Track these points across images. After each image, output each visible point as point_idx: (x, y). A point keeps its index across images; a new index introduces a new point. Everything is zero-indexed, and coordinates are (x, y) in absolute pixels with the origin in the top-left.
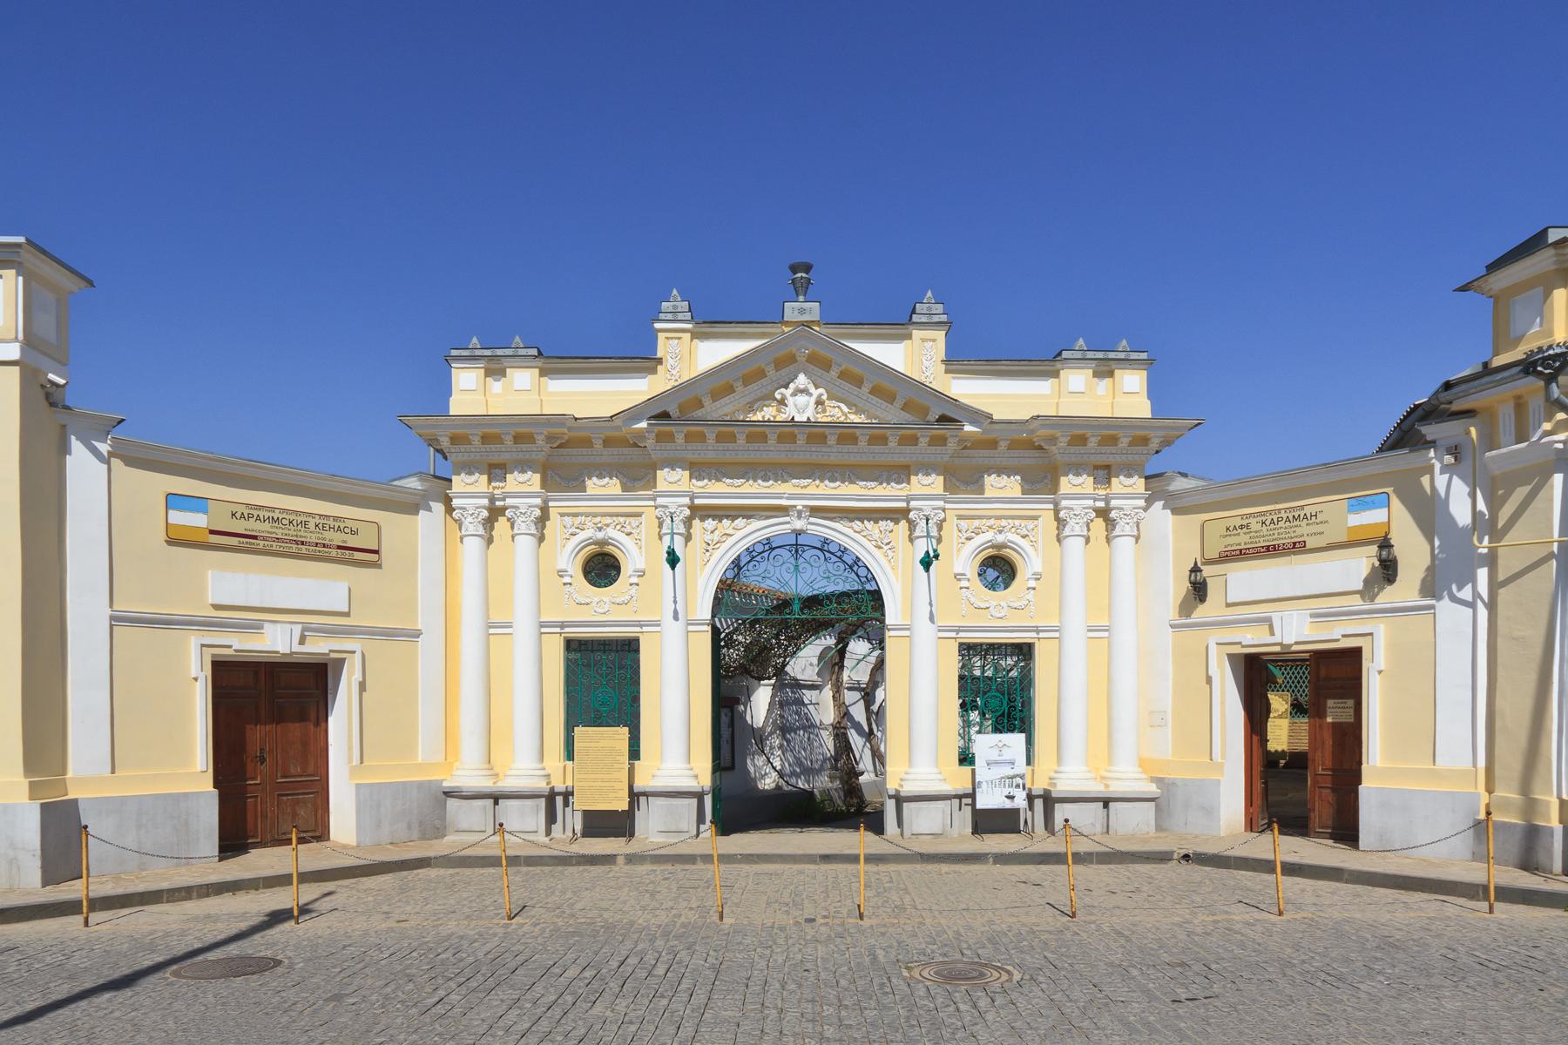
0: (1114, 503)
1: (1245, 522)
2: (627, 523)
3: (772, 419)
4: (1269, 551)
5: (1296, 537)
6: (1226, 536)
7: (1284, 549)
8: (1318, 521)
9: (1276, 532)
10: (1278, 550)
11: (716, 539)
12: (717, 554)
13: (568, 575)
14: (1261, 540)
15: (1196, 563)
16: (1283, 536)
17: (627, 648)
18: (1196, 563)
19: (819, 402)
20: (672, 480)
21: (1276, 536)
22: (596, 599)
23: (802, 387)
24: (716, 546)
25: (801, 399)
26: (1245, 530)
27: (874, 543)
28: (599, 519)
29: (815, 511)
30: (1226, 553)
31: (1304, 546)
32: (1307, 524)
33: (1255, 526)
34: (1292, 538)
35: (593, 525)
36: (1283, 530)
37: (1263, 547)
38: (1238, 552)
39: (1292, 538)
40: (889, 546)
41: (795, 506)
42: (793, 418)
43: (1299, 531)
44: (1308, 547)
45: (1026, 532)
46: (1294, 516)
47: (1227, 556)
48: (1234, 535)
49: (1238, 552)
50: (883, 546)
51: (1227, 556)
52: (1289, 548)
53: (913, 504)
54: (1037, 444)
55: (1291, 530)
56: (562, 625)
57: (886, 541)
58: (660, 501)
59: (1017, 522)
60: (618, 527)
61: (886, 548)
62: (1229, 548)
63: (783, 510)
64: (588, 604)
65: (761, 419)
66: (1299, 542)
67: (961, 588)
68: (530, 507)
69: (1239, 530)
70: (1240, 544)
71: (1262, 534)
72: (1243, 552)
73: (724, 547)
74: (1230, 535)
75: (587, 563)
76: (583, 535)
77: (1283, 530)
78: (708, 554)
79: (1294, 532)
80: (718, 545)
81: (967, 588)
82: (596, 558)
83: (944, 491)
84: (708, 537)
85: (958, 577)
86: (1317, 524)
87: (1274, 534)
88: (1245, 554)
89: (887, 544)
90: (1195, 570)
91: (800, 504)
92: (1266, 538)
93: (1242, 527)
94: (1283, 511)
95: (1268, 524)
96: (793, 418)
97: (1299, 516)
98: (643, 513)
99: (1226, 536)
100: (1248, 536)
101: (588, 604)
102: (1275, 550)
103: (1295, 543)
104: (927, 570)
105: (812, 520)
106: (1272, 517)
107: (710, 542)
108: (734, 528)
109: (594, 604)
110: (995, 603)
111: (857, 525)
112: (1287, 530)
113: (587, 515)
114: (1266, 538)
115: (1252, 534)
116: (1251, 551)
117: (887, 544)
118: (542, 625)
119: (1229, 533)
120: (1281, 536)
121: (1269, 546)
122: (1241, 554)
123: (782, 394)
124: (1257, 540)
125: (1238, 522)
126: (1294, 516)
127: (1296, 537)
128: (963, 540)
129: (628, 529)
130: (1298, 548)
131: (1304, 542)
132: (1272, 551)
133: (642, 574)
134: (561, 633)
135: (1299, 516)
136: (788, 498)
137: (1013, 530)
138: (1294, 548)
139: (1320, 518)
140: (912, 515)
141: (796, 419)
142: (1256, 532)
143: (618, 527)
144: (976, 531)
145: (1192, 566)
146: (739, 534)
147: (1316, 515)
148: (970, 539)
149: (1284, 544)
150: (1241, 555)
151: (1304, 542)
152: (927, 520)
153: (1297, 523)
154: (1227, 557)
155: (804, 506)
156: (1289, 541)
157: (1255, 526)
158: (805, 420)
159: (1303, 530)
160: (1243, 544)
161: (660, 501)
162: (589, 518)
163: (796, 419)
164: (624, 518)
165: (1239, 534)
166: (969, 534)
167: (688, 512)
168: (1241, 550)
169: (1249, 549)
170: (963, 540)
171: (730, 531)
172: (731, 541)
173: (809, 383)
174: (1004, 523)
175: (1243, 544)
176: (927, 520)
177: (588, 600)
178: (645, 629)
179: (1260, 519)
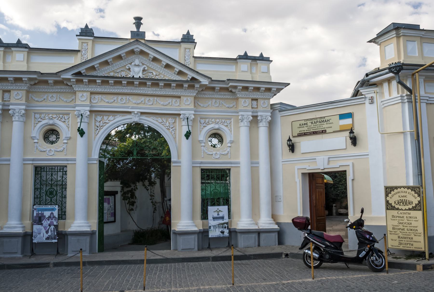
0: (259, 114)
1: (306, 122)
2: (63, 117)
3: (125, 76)
4: (314, 133)
5: (323, 128)
6: (300, 127)
7: (319, 133)
8: (330, 123)
9: (316, 126)
10: (317, 133)
11: (101, 125)
12: (102, 131)
13: (36, 139)
14: (311, 129)
15: (289, 138)
16: (319, 128)
17: (62, 170)
18: (289, 138)
19: (144, 70)
20: (82, 100)
21: (316, 128)
22: (48, 149)
23: (137, 64)
24: (101, 128)
25: (137, 69)
26: (306, 125)
27: (166, 127)
28: (51, 115)
29: (142, 113)
31: (326, 132)
32: (326, 124)
33: (309, 124)
34: (322, 129)
35: (48, 118)
36: (318, 126)
37: (312, 132)
38: (304, 134)
39: (322, 129)
40: (172, 129)
41: (134, 112)
42: (133, 76)
43: (324, 126)
44: (327, 132)
45: (227, 125)
46: (322, 121)
47: (300, 135)
48: (302, 127)
49: (304, 134)
50: (170, 129)
51: (300, 135)
52: (321, 133)
53: (181, 112)
54: (230, 90)
55: (321, 126)
56: (33, 160)
57: (171, 127)
58: (77, 108)
59: (223, 121)
60: (59, 119)
61: (171, 130)
62: (301, 132)
63: (130, 113)
64: (45, 151)
65: (120, 76)
66: (324, 130)
67: (202, 146)
68: (20, 109)
69: (304, 125)
70: (304, 131)
71: (311, 127)
72: (306, 133)
73: (105, 128)
74: (301, 127)
75: (46, 133)
76: (44, 122)
77: (318, 126)
78: (97, 131)
79: (322, 126)
80: (102, 127)
81: (204, 146)
82: (50, 132)
83: (194, 107)
84: (98, 124)
85: (200, 142)
86: (330, 124)
87: (315, 127)
88: (306, 134)
89: (172, 128)
90: (289, 140)
91: (136, 111)
92: (313, 129)
93: (305, 124)
94: (318, 119)
95: (313, 123)
96: (133, 76)
97: (324, 120)
98: (70, 113)
99: (300, 127)
100: (307, 128)
101: (45, 151)
102: (316, 133)
103: (322, 131)
104: (187, 138)
105: (141, 117)
106: (315, 121)
107: (99, 126)
108: (109, 120)
109: (47, 152)
110: (214, 153)
111: (160, 120)
112: (320, 126)
113: (46, 114)
114: (313, 129)
116: (308, 133)
117: (172, 128)
118: (24, 160)
119: (300, 126)
120: (318, 128)
121: (314, 132)
123: (128, 66)
124: (310, 129)
125: (303, 122)
126: (322, 121)
127: (323, 128)
128: (202, 127)
129: (63, 120)
130: (324, 132)
131: (326, 130)
132: (315, 133)
133: (69, 139)
134: (32, 164)
135: (324, 120)
136: (131, 108)
137: (222, 123)
138: (322, 132)
139: (331, 121)
140: (181, 116)
141: (135, 77)
142: (310, 126)
143: (59, 119)
144: (207, 123)
145: (288, 138)
146: (111, 123)
147: (329, 121)
148: (205, 127)
149: (319, 131)
150: (305, 134)
151: (326, 130)
152: (188, 119)
153: (323, 123)
154: (300, 135)
155: (138, 112)
156: (320, 130)
157: (309, 124)
158: (138, 77)
159: (325, 126)
160: (305, 131)
161: (77, 108)
162: (47, 115)
163: (135, 77)
164: (62, 115)
165: (304, 127)
166: (204, 125)
167: (88, 113)
168: (305, 133)
169: (307, 132)
170: (202, 127)
171: (107, 121)
172: (108, 125)
173: (140, 63)
174: (218, 120)
175: (305, 131)
176: (188, 119)
177: (45, 150)
178: (69, 162)
179: (311, 121)
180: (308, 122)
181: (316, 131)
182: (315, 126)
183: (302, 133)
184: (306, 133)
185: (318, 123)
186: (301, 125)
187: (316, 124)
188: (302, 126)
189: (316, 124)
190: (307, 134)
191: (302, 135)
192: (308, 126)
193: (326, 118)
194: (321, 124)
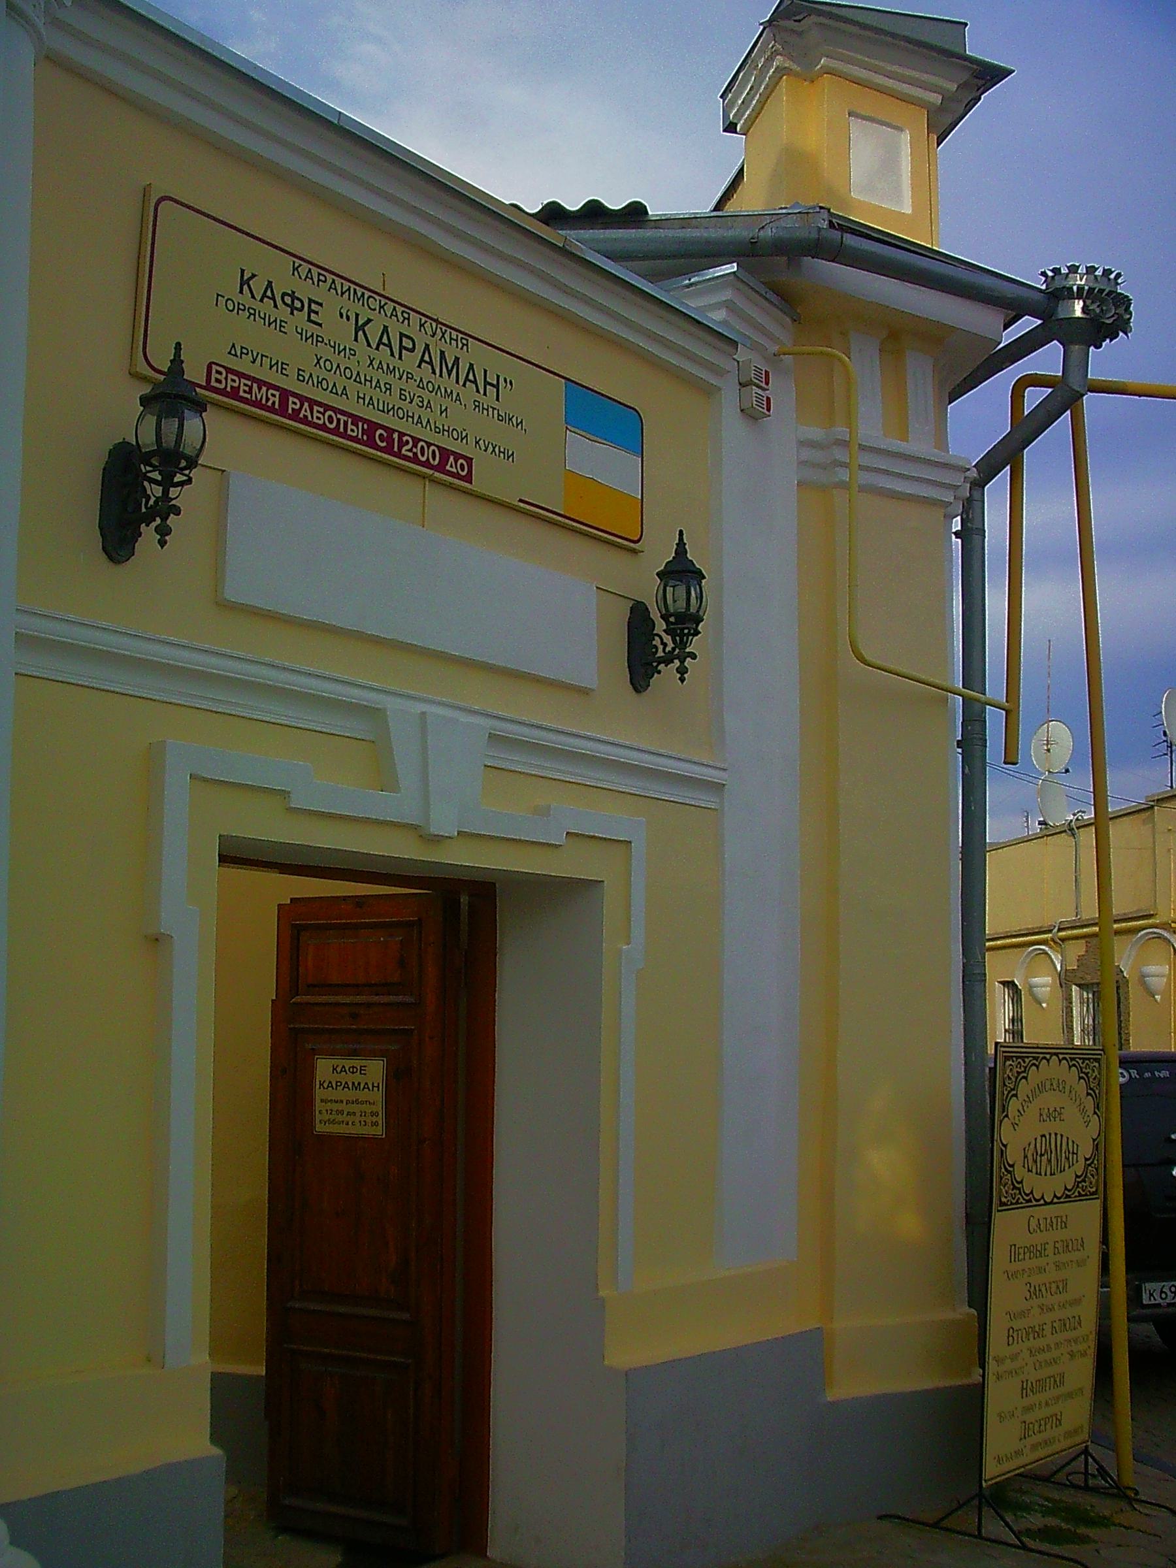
1: (305, 291)
7: (414, 461)
21: (394, 400)
30: (232, 382)
37: (356, 419)
47: (234, 394)
51: (234, 394)
52: (426, 464)
55: (437, 401)
77: (411, 386)
88: (295, 416)
93: (292, 302)
102: (388, 450)
103: (445, 453)
114: (366, 390)
115: (326, 352)
121: (373, 426)
122: (283, 411)
124: (341, 382)
149: (416, 441)
151: (469, 460)
153: (447, 382)
160: (292, 372)
165: (281, 326)
168: (285, 394)
169: (313, 403)
180: (332, 304)
181: (390, 431)
182: (377, 375)
183: (261, 383)
184: (302, 399)
185: (410, 361)
186: (258, 286)
187: (394, 362)
188: (256, 305)
189: (394, 362)
190: (305, 421)
191: (257, 404)
192: (319, 340)
193: (474, 354)
194: (437, 380)
